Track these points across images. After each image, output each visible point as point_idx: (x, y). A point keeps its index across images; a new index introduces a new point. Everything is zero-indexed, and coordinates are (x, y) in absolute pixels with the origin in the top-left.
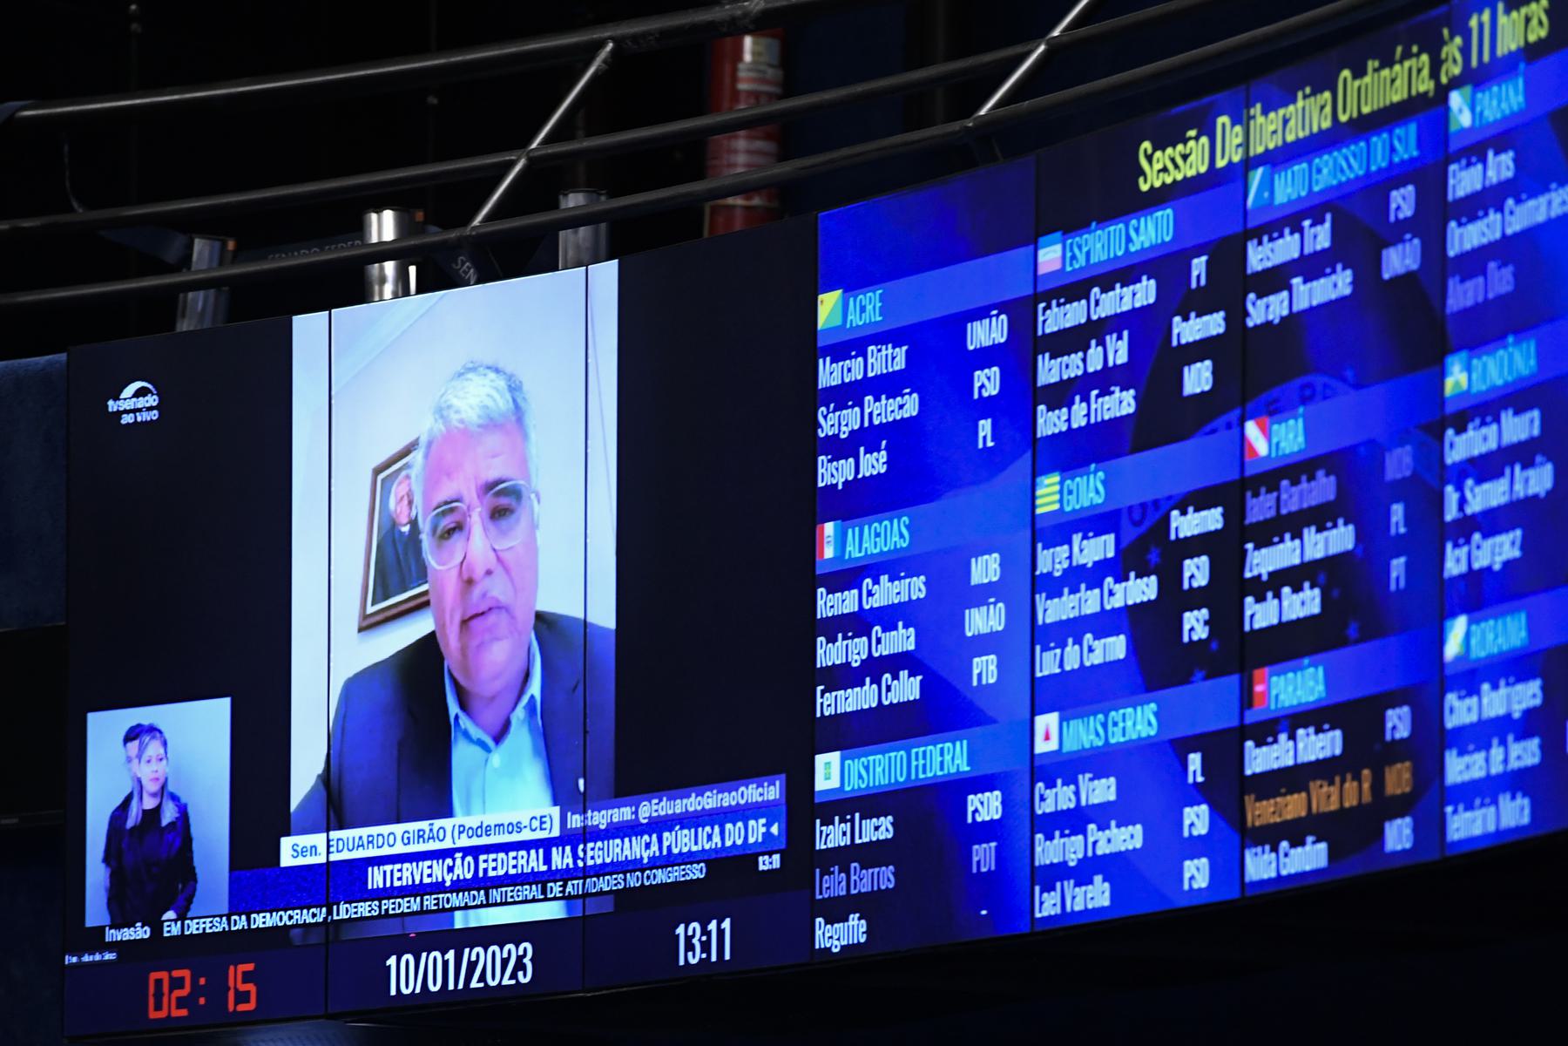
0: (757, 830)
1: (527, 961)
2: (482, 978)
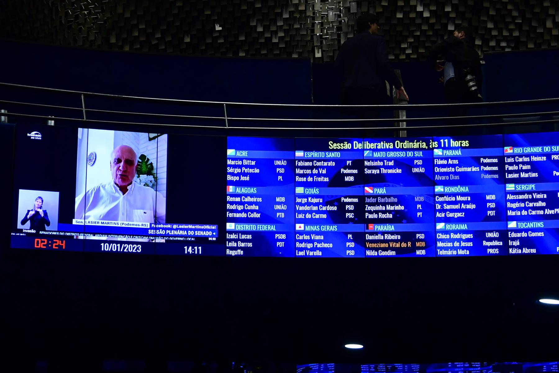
0: (210, 233)
1: (140, 248)
2: (128, 249)
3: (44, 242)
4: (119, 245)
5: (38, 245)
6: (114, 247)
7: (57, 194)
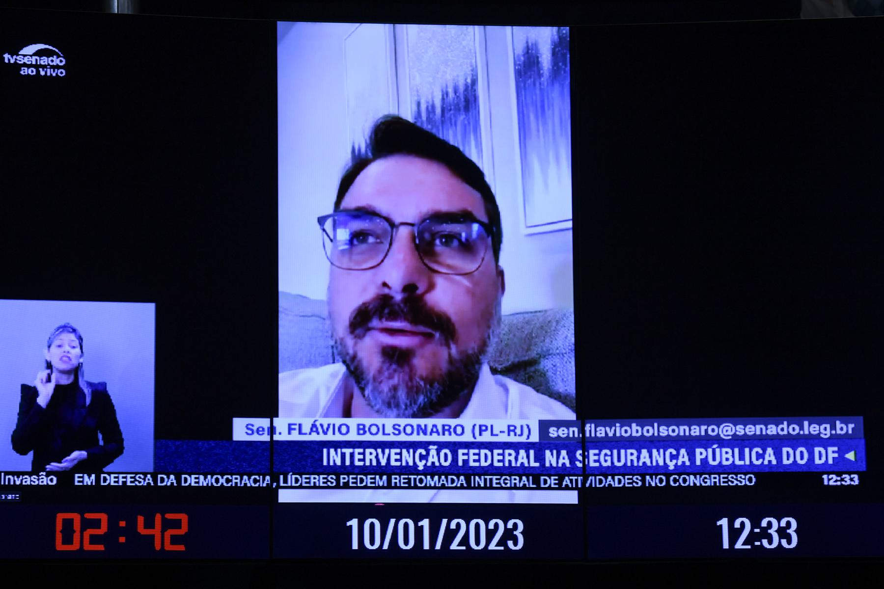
1: (518, 533)
2: (465, 541)
3: (96, 524)
4: (425, 523)
5: (67, 540)
6: (405, 534)
7: (149, 309)
